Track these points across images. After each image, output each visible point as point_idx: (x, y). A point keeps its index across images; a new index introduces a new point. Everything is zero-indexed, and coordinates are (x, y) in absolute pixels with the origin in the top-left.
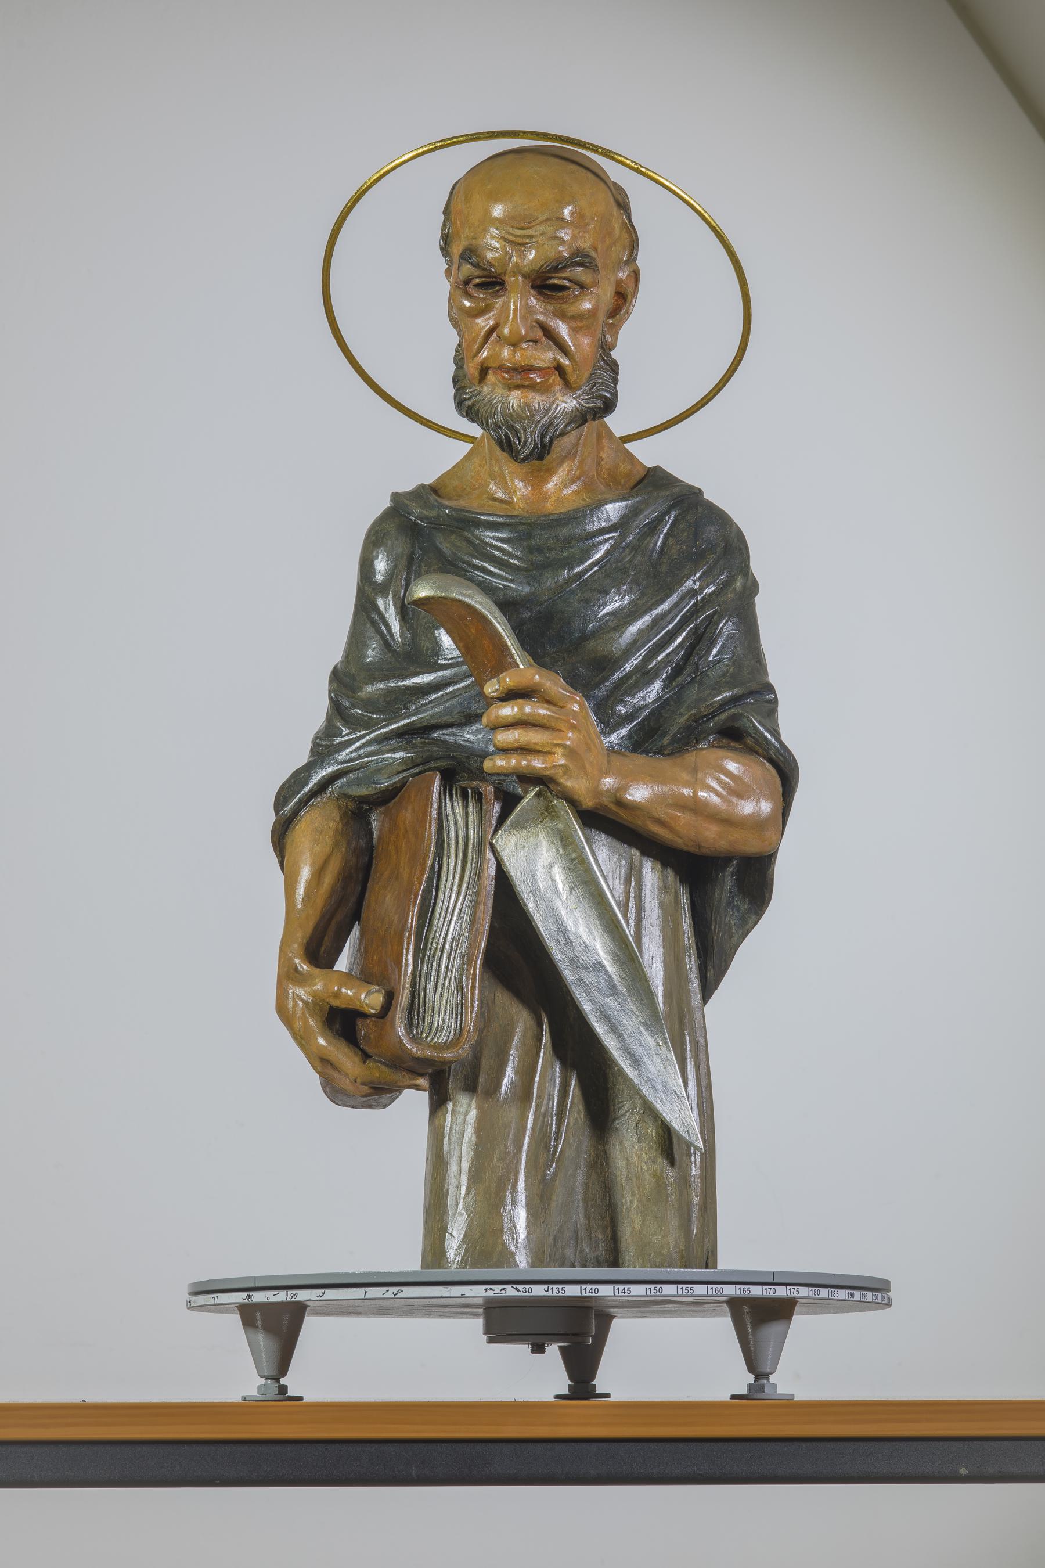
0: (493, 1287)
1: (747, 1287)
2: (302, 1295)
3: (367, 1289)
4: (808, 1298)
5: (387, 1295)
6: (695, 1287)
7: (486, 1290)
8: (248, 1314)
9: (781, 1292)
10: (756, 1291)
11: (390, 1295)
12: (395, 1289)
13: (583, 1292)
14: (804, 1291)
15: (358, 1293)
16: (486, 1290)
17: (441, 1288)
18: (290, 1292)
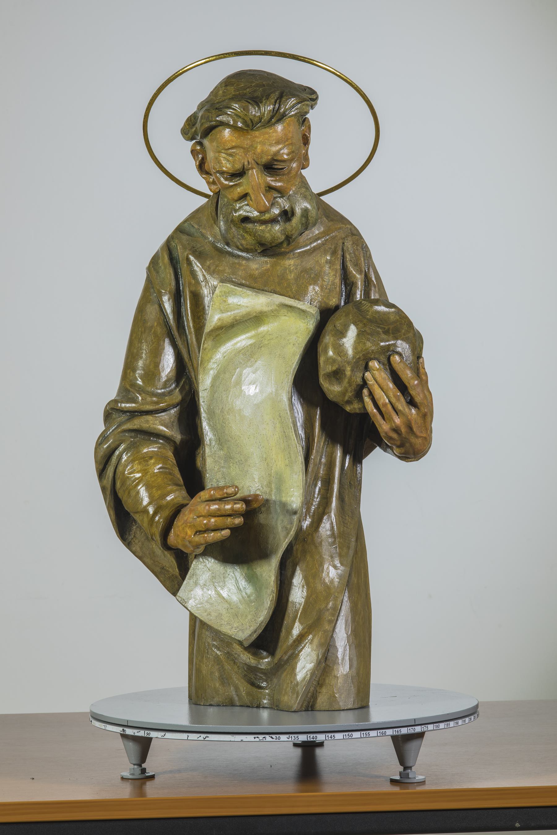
0: (259, 736)
1: (399, 729)
2: (153, 734)
3: (190, 735)
4: (434, 730)
5: (200, 739)
7: (255, 738)
9: (418, 729)
10: (404, 731)
11: (201, 738)
12: (203, 736)
13: (309, 738)
14: (431, 727)
15: (184, 736)
16: (255, 738)
18: (146, 732)
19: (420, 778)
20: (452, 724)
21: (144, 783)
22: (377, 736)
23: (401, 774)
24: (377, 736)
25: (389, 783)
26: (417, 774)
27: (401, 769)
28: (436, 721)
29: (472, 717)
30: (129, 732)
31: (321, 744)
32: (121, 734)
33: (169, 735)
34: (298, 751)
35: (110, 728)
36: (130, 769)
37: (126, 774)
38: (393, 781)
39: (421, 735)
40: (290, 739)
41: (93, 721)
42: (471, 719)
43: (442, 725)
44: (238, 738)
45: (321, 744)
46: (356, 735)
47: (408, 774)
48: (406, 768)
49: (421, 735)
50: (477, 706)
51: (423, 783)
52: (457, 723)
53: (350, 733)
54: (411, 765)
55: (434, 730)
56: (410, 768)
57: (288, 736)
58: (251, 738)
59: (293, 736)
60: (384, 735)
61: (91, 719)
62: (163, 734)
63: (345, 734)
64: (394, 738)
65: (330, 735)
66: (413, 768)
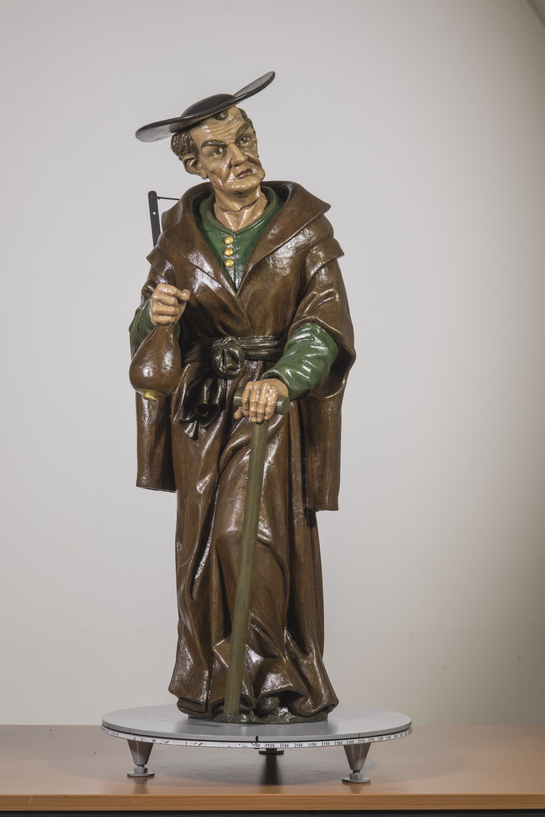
3: (187, 742)
4: (378, 741)
5: (196, 745)
6: (330, 742)
8: (132, 744)
9: (367, 740)
11: (197, 745)
14: (376, 739)
15: (183, 743)
17: (220, 743)
19: (365, 779)
20: (392, 737)
21: (146, 780)
22: (335, 745)
23: (350, 776)
24: (335, 745)
25: (341, 782)
26: (365, 775)
27: (351, 772)
28: (380, 735)
29: (408, 732)
30: (138, 739)
31: (281, 753)
32: (129, 741)
33: (171, 742)
34: (263, 758)
35: (121, 735)
36: (135, 769)
37: (132, 772)
38: (344, 782)
39: (367, 746)
40: (267, 747)
41: (106, 729)
42: (406, 733)
43: (385, 738)
44: (226, 745)
45: (281, 753)
46: (319, 744)
47: (357, 776)
48: (355, 772)
49: (367, 746)
50: (410, 724)
51: (368, 783)
52: (396, 736)
53: (314, 742)
54: (359, 769)
55: (378, 741)
56: (358, 771)
57: (266, 744)
58: (237, 745)
59: (270, 744)
60: (340, 744)
61: (104, 728)
62: (166, 740)
63: (310, 743)
64: (346, 747)
65: (298, 744)
66: (361, 771)
